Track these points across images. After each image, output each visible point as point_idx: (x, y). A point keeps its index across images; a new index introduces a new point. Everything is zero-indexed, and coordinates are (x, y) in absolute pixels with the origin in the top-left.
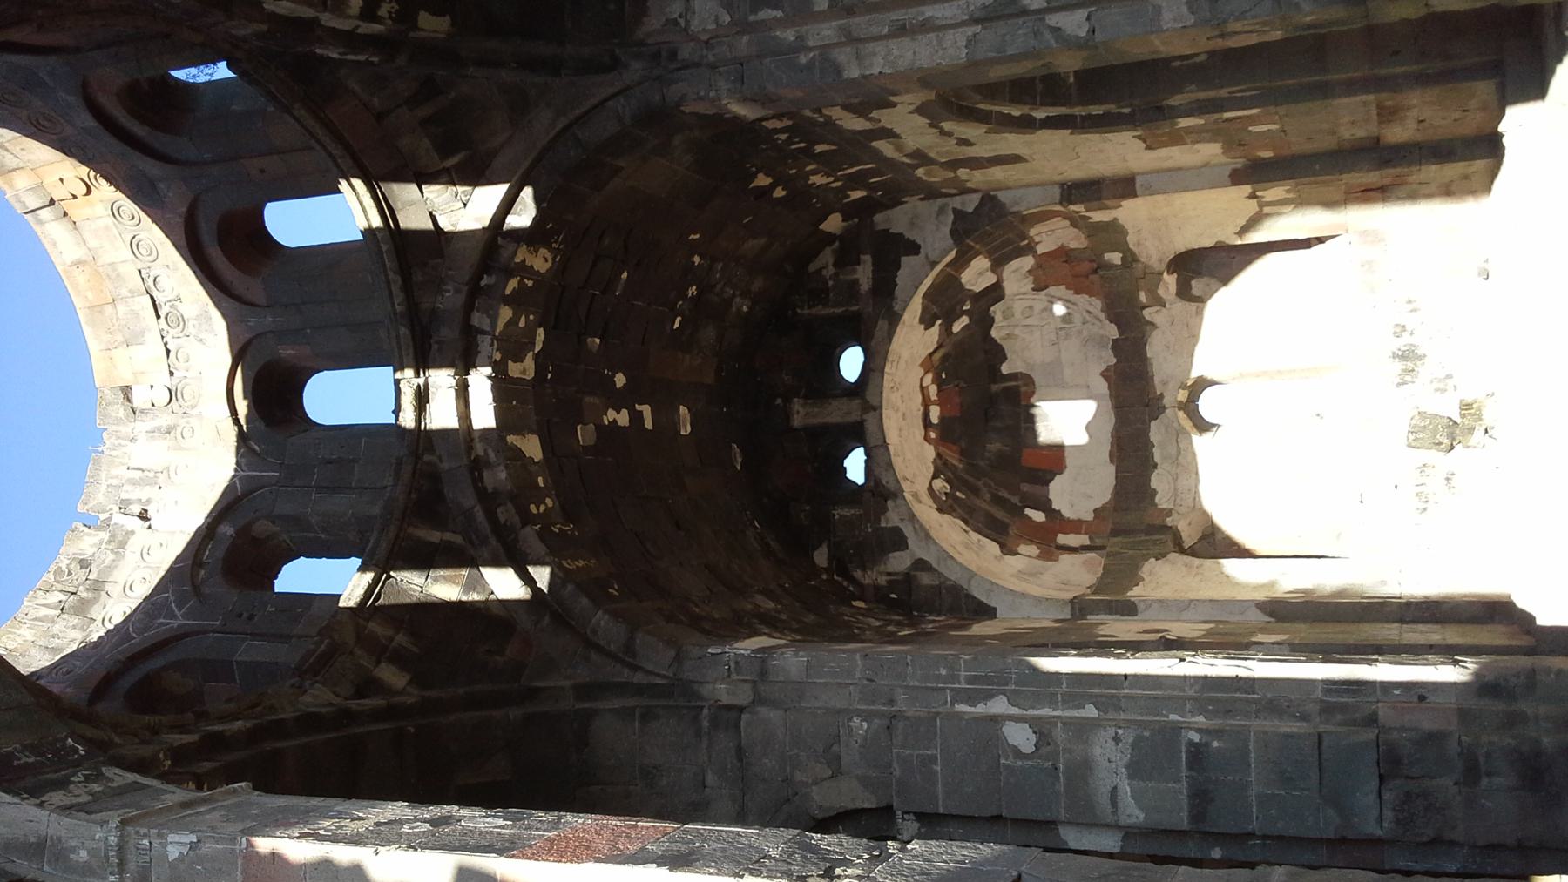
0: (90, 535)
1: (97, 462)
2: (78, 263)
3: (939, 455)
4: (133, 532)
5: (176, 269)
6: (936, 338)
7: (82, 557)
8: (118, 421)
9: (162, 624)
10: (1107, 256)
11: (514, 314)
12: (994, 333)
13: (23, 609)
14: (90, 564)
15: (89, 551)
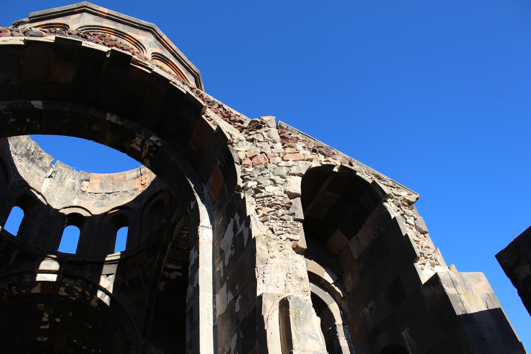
0: (49, 162)
1: (70, 168)
2: (125, 177)
4: (46, 173)
5: (117, 201)
7: (43, 158)
8: (80, 176)
9: (14, 175)
11: (79, 292)
13: (32, 141)
14: (40, 160)
15: (44, 161)
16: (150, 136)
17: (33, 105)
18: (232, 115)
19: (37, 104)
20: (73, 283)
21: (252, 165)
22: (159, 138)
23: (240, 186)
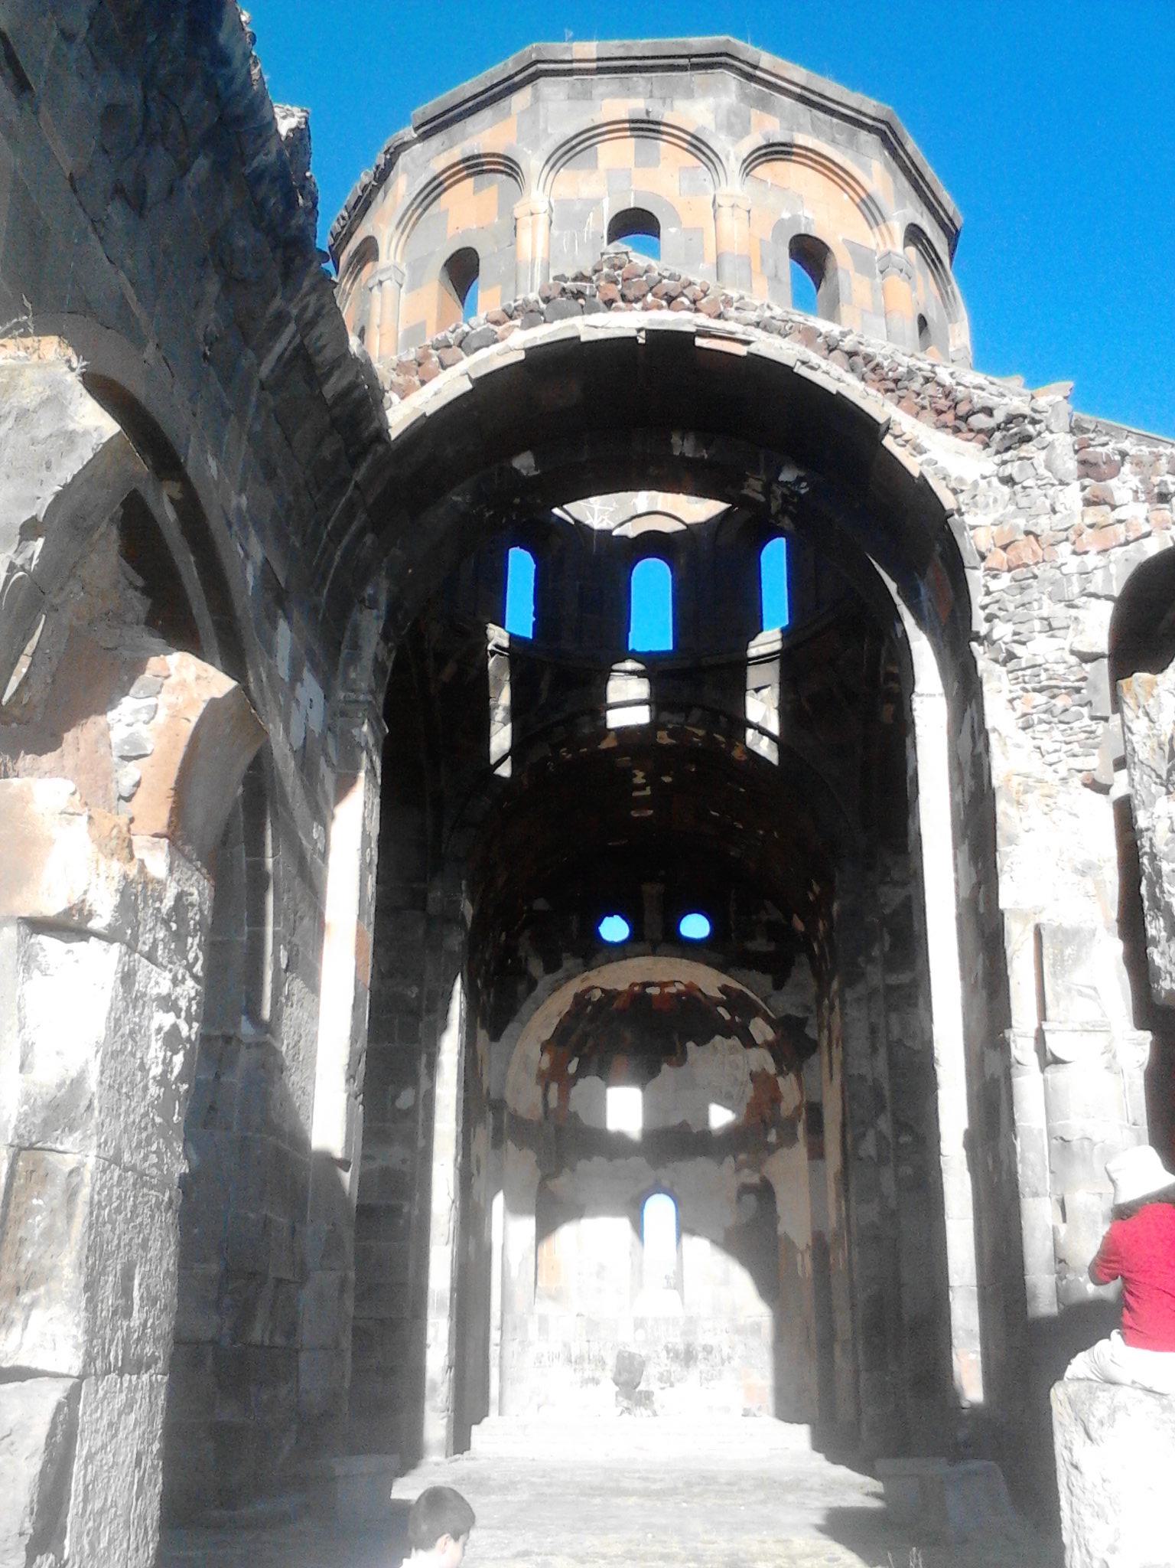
3: (620, 993)
6: (712, 994)
10: (774, 1131)
12: (718, 1038)
16: (779, 472)
17: (517, 471)
18: (960, 396)
19: (524, 463)
20: (682, 720)
21: (1006, 567)
22: (799, 468)
23: (978, 633)
